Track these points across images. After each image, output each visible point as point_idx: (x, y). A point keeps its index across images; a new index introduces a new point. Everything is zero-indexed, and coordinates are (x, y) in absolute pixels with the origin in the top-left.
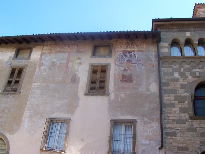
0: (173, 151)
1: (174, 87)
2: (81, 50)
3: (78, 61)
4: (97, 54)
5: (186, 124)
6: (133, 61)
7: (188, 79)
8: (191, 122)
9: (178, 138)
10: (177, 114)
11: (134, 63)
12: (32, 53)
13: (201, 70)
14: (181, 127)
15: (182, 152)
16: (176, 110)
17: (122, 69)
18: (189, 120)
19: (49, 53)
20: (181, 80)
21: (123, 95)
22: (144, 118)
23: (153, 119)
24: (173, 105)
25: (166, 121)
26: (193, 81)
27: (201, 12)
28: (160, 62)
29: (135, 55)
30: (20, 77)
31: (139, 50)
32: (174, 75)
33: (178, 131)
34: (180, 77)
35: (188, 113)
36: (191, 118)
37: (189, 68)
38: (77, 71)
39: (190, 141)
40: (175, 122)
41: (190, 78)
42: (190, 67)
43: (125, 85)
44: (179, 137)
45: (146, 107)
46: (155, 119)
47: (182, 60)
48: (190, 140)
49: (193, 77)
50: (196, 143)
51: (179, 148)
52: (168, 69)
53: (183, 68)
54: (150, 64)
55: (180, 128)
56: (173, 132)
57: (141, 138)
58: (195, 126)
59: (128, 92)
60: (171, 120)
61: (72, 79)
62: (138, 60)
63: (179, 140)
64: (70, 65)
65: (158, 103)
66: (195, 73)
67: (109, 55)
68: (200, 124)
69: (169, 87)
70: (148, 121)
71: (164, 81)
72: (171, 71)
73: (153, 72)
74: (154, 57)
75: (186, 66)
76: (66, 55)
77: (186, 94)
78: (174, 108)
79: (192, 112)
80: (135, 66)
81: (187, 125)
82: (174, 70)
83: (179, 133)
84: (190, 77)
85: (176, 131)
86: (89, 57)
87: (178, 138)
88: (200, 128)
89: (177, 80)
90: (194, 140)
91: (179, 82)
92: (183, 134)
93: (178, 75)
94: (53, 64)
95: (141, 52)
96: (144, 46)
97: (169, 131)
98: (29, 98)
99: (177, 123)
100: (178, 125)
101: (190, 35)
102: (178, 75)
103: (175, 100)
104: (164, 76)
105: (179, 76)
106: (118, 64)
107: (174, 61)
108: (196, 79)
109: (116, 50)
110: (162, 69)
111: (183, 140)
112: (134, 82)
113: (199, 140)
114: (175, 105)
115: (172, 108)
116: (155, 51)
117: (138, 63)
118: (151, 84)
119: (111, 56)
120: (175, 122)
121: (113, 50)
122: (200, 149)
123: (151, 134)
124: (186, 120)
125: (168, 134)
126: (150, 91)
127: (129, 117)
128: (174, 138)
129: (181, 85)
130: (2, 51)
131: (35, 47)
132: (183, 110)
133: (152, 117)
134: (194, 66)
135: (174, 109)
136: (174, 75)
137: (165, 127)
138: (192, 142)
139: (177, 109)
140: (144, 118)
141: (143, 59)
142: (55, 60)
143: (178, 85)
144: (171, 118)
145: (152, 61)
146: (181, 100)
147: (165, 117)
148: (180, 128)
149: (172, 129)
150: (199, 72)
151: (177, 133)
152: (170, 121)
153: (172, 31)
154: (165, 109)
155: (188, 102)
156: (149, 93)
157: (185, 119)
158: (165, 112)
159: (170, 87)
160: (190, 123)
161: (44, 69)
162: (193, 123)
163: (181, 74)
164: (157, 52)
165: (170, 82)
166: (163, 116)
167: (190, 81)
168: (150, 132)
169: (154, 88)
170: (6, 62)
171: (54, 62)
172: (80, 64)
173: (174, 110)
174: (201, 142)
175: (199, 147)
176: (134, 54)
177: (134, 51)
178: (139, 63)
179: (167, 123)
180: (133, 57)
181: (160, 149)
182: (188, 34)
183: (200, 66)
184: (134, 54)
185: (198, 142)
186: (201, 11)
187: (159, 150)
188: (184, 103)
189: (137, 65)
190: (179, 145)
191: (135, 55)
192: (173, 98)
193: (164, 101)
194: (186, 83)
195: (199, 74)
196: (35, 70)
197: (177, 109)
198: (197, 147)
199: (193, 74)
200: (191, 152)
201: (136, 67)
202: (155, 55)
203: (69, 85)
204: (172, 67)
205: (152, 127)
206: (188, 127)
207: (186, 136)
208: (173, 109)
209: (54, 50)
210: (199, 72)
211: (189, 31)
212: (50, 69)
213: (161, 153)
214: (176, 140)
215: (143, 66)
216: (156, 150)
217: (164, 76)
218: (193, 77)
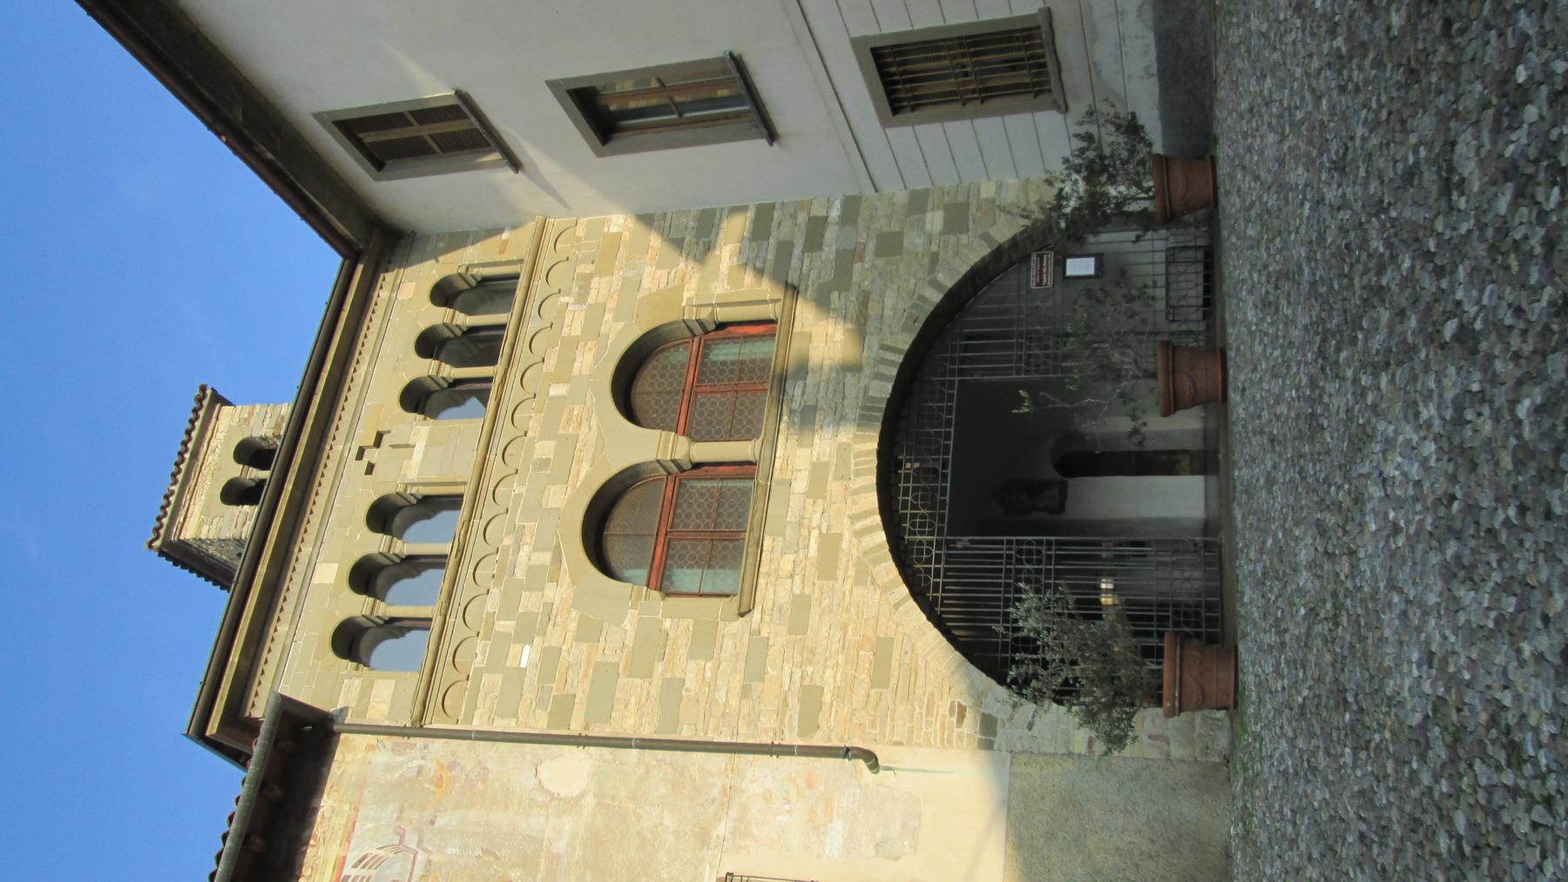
0: (892, 706)
1: (586, 671)
5: (768, 638)
7: (557, 602)
8: (763, 611)
9: (829, 679)
10: (715, 676)
11: (409, 867)
13: (527, 538)
14: (779, 663)
15: (894, 663)
16: (697, 674)
18: (754, 620)
20: (554, 638)
22: (714, 834)
23: (725, 793)
24: (673, 687)
25: (743, 730)
26: (573, 583)
27: (206, 528)
28: (435, 726)
29: (361, 861)
31: (341, 831)
32: (525, 669)
33: (797, 676)
34: (538, 640)
35: (721, 624)
37: (505, 595)
39: (850, 628)
40: (754, 685)
41: (557, 593)
42: (497, 585)
44: (829, 672)
45: (661, 824)
46: (728, 781)
48: (844, 628)
49: (555, 579)
50: (861, 604)
51: (880, 677)
52: (486, 694)
53: (499, 619)
54: (439, 784)
55: (787, 668)
56: (802, 702)
57: (818, 857)
58: (783, 597)
60: (743, 702)
63: (839, 676)
65: (649, 755)
66: (532, 570)
68: (778, 577)
69: (581, 696)
70: (734, 813)
71: (540, 725)
72: (499, 677)
73: (485, 768)
74: (400, 759)
75: (492, 603)
77: (626, 622)
78: (688, 684)
80: (429, 862)
81: (778, 638)
82: (495, 665)
83: (810, 669)
85: (797, 686)
87: (831, 680)
88: (797, 579)
89: (550, 657)
90: (848, 610)
91: (565, 648)
92: (813, 652)
93: (527, 648)
95: (357, 824)
97: (796, 717)
99: (761, 676)
100: (771, 672)
101: (336, 566)
102: (527, 648)
104: (515, 715)
105: (531, 642)
107: (450, 658)
108: (565, 564)
110: (477, 724)
111: (841, 659)
113: (848, 587)
114: (671, 680)
115: (683, 693)
116: (370, 748)
117: (414, 847)
118: (547, 785)
120: (754, 685)
122: (886, 588)
124: (752, 633)
125: (809, 722)
126: (581, 796)
128: (827, 698)
129: (578, 638)
132: (704, 644)
133: (715, 793)
134: (502, 570)
136: (523, 665)
137: (771, 734)
138: (854, 617)
139: (692, 672)
140: (718, 836)
141: (399, 818)
143: (574, 653)
144: (734, 702)
145: (420, 769)
147: (725, 729)
148: (787, 668)
149: (785, 700)
150: (536, 549)
151: (806, 682)
152: (745, 711)
153: (285, 650)
154: (685, 727)
155: (665, 616)
156: (590, 801)
157: (746, 640)
158: (700, 726)
159: (581, 691)
160: (767, 618)
162: (769, 605)
163: (527, 630)
164: (381, 737)
165: (554, 693)
166: (717, 739)
167: (572, 596)
168: (789, 812)
173: (697, 682)
174: (858, 582)
175: (878, 592)
176: (355, 866)
177: (341, 863)
178: (416, 839)
180: (373, 872)
183: (507, 541)
184: (355, 866)
185: (855, 590)
186: (200, 527)
187: (882, 773)
188: (671, 635)
189: (426, 851)
191: (365, 857)
192: (638, 681)
193: (647, 732)
194: (573, 614)
195: (546, 550)
197: (692, 672)
198: (877, 597)
199: (538, 578)
200: (900, 629)
201: (435, 858)
202: (396, 750)
204: (480, 671)
205: (767, 797)
206: (783, 629)
207: (824, 642)
208: (688, 690)
210: (536, 549)
211: (311, 567)
213: (895, 763)
214: (839, 688)
215: (440, 822)
216: (881, 784)
217: (515, 715)
218: (555, 579)
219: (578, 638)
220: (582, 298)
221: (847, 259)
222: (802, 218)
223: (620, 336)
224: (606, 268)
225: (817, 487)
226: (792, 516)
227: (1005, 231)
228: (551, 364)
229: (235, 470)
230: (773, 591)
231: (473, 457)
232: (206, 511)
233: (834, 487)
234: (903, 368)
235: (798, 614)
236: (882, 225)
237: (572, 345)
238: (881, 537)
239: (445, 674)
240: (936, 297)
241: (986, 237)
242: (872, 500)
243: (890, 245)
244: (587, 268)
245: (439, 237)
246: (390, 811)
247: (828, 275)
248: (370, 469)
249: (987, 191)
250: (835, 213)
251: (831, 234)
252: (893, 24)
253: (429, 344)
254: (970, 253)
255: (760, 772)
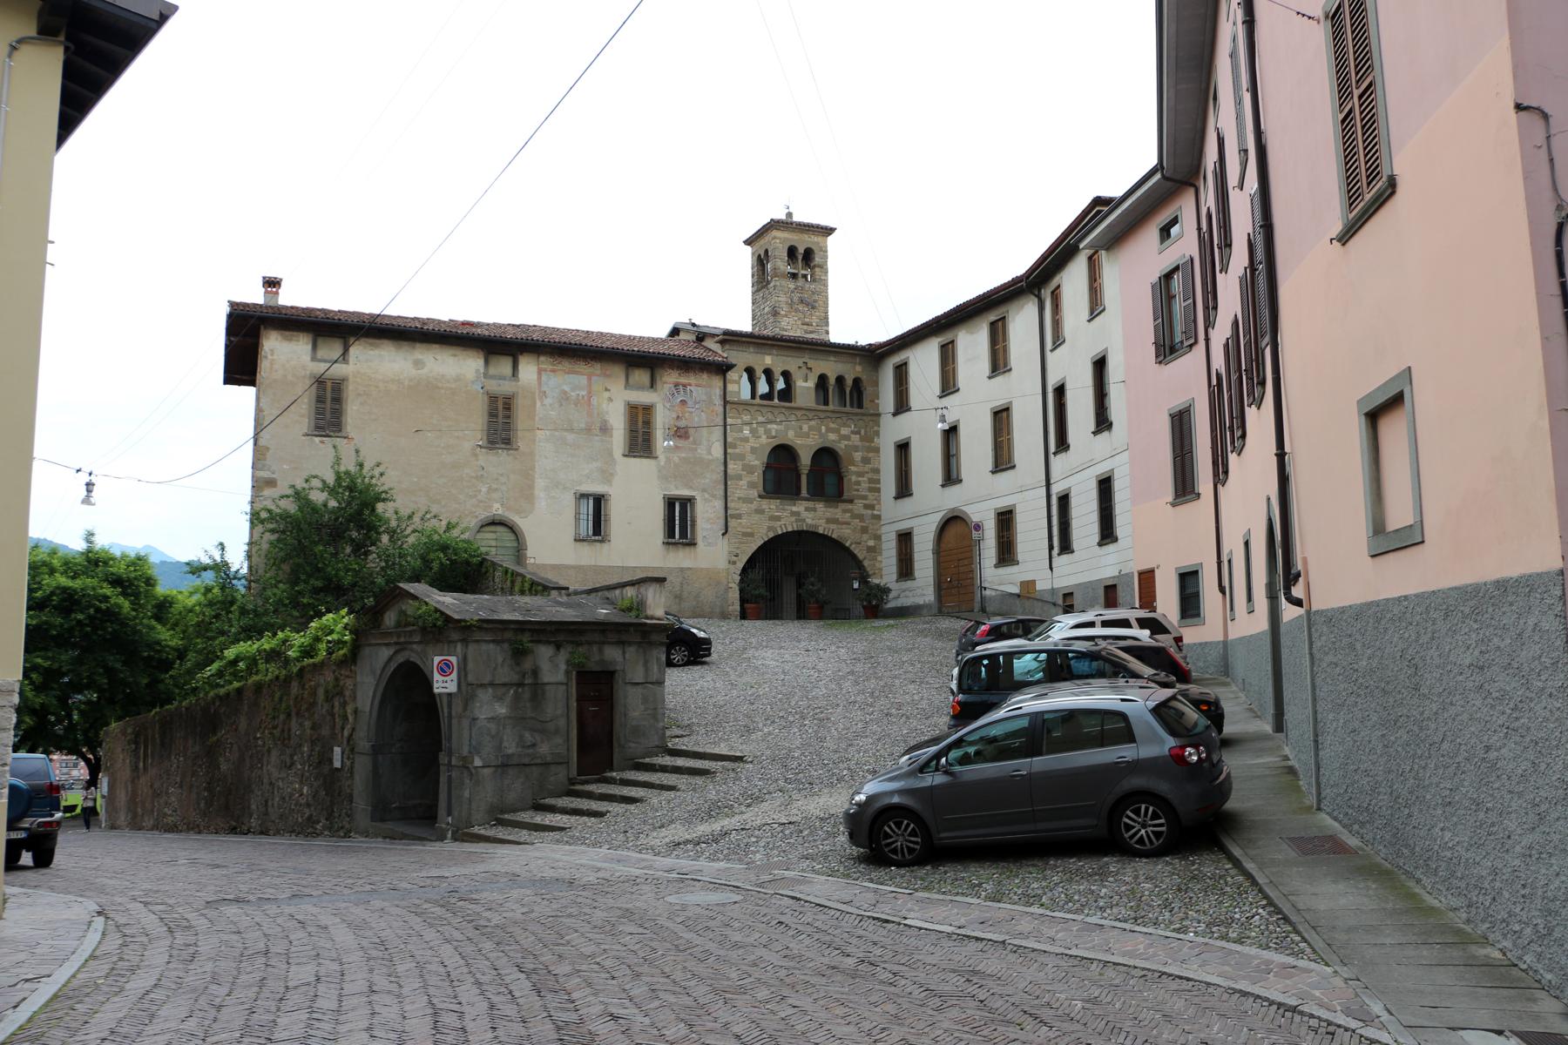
2: (608, 373)
3: (606, 394)
4: (631, 380)
6: (690, 403)
9: (743, 521)
12: (520, 367)
17: (675, 416)
19: (553, 371)
21: (676, 459)
24: (739, 478)
26: (767, 444)
30: (509, 417)
36: (760, 496)
38: (607, 413)
41: (764, 439)
43: (681, 443)
47: (756, 408)
51: (745, 534)
58: (764, 507)
59: (683, 455)
61: (601, 429)
62: (696, 403)
64: (594, 401)
65: (722, 474)
66: (770, 430)
67: (652, 387)
69: (737, 451)
71: (729, 440)
75: (761, 419)
76: (583, 380)
79: (761, 488)
81: (754, 506)
84: (764, 437)
86: (623, 387)
89: (746, 440)
94: (564, 398)
96: (705, 376)
98: (537, 457)
99: (744, 502)
103: (743, 470)
106: (668, 405)
109: (664, 379)
112: (691, 439)
119: (656, 391)
121: (658, 378)
123: (712, 516)
125: (733, 516)
127: (685, 492)
129: (752, 447)
130: (455, 356)
131: (521, 354)
132: (752, 485)
135: (741, 483)
139: (743, 483)
142: (566, 388)
143: (748, 446)
146: (749, 469)
156: (710, 457)
159: (737, 451)
161: (551, 405)
163: (753, 431)
169: (717, 451)
170: (473, 382)
171: (565, 392)
172: (610, 400)
177: (690, 385)
179: (732, 501)
181: (723, 535)
182: (768, 360)
190: (744, 530)
196: (535, 403)
197: (743, 483)
199: (767, 432)
203: (597, 438)
209: (560, 367)
212: (561, 405)
219: (752, 447)
220: (853, 432)
221: (861, 517)
222: (875, 502)
223: (841, 447)
224: (862, 439)
225: (793, 514)
226: (786, 507)
227: (866, 563)
228: (832, 425)
229: (801, 250)
230: (765, 504)
231: (803, 405)
232: (786, 240)
233: (793, 519)
234: (827, 536)
235: (760, 511)
236: (871, 527)
237: (837, 431)
238: (780, 533)
239: (741, 408)
240: (847, 545)
241: (865, 558)
242: (790, 529)
243: (864, 530)
244: (863, 432)
245: (877, 377)
246: (704, 397)
247: (856, 512)
248: (800, 367)
249: (879, 558)
250: (875, 512)
251: (869, 512)
252: (916, 539)
253: (840, 380)
254: (860, 553)
255: (719, 504)
